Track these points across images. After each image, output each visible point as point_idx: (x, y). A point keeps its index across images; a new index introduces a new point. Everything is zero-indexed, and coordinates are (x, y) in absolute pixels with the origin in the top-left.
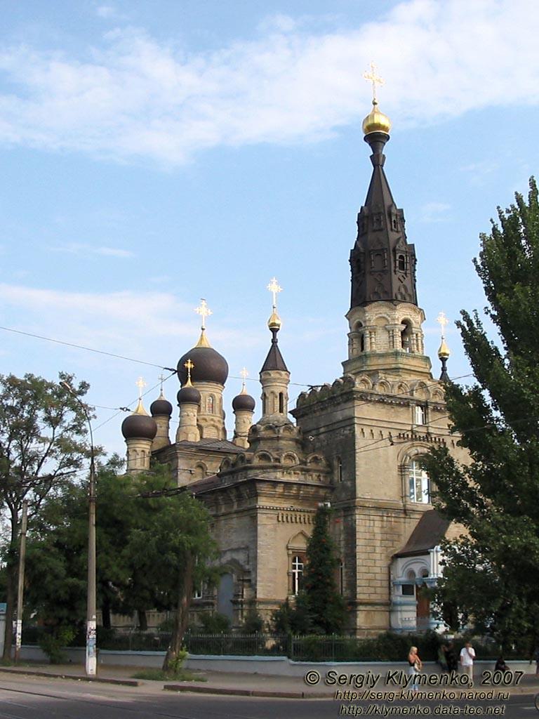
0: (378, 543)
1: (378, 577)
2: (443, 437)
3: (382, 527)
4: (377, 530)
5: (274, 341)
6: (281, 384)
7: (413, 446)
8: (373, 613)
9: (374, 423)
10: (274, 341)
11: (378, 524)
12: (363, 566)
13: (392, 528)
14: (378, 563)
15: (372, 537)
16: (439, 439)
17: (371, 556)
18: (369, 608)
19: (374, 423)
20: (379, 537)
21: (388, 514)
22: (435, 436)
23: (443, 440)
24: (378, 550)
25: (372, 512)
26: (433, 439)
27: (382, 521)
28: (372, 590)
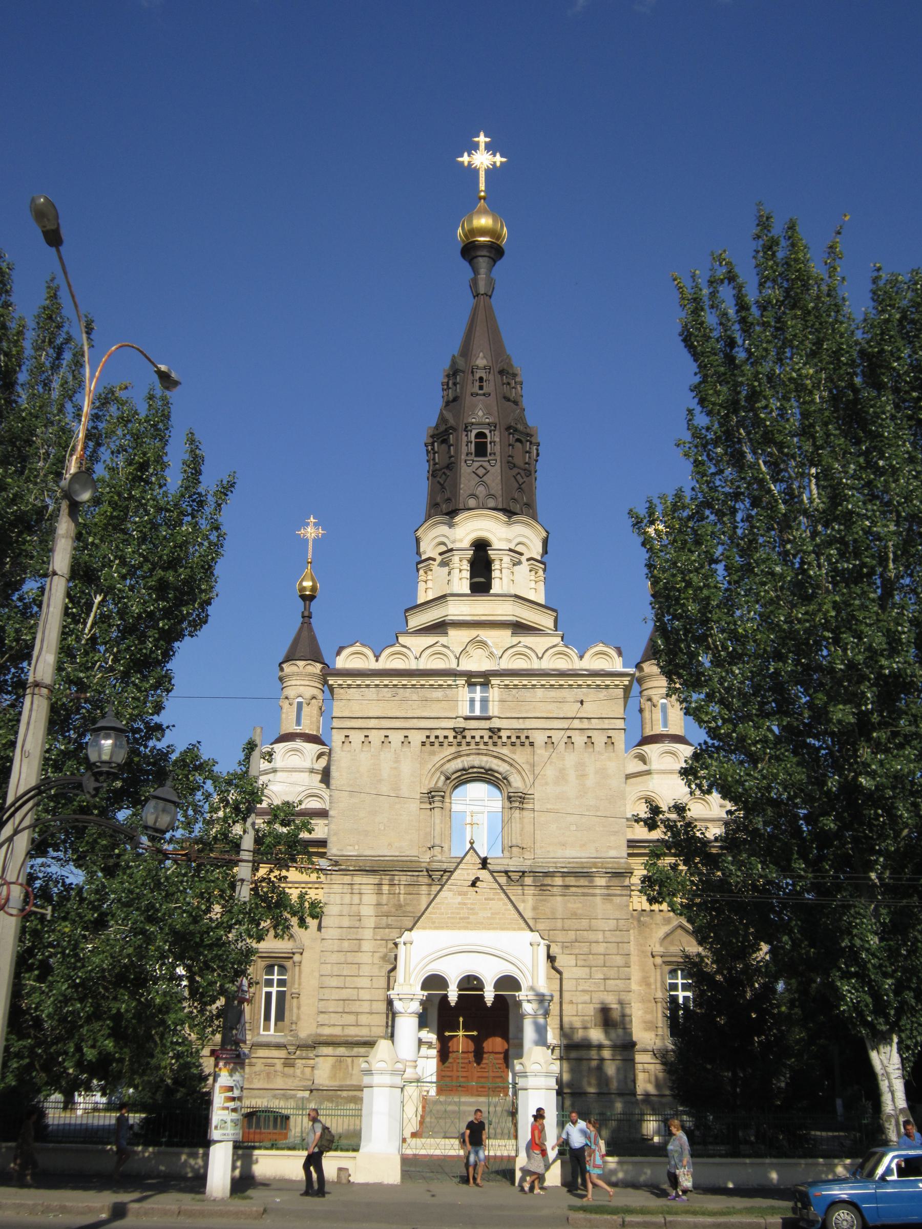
0: (368, 934)
1: (365, 995)
2: (530, 733)
3: (379, 904)
4: (367, 910)
5: (307, 617)
6: (298, 683)
7: (458, 755)
8: (349, 1060)
9: (372, 723)
10: (307, 617)
11: (370, 898)
12: (332, 976)
13: (399, 906)
14: (365, 970)
15: (357, 924)
17: (350, 957)
18: (341, 1051)
19: (372, 723)
20: (370, 922)
21: (393, 880)
22: (508, 733)
23: (527, 737)
24: (367, 946)
25: (358, 879)
26: (504, 739)
27: (380, 893)
28: (351, 1019)
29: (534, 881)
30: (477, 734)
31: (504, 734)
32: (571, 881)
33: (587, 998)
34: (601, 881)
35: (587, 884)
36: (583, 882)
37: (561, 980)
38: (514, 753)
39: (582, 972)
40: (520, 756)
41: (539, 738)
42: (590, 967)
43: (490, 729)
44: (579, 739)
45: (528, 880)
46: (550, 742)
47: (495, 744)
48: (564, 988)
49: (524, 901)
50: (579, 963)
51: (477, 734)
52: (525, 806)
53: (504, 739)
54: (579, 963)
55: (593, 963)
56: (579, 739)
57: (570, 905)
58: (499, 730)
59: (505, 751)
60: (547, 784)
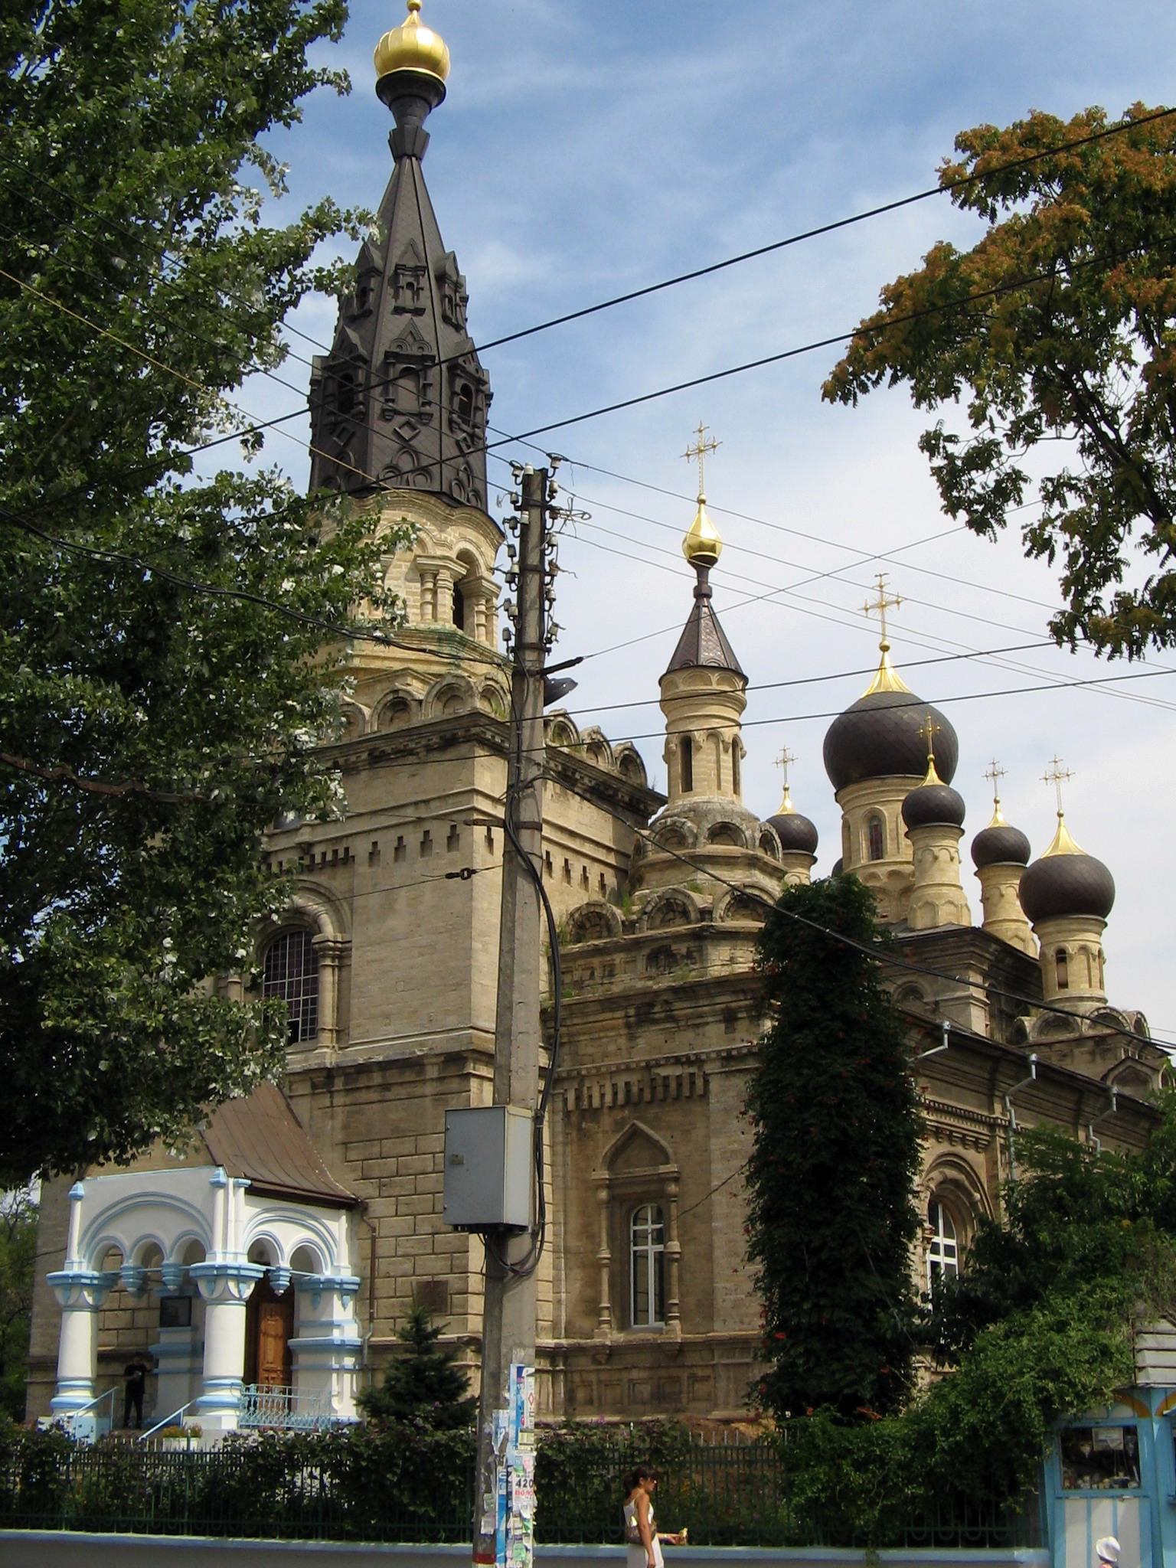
16: (335, 852)
23: (347, 850)
26: (318, 859)
29: (346, 1083)
30: (284, 858)
31: (318, 851)
32: (393, 1076)
33: (408, 1266)
34: (432, 1072)
35: (413, 1078)
36: (409, 1076)
37: (374, 1239)
38: (334, 878)
39: (401, 1224)
40: (336, 882)
41: (361, 848)
42: (415, 1215)
43: (300, 845)
44: (413, 839)
45: (339, 1083)
46: (374, 855)
47: (310, 868)
48: (380, 1251)
49: (332, 1117)
50: (402, 1209)
51: (284, 858)
52: (346, 962)
53: (318, 859)
54: (402, 1209)
55: (419, 1209)
56: (413, 839)
57: (392, 1116)
58: (310, 845)
59: (322, 879)
60: (368, 920)
